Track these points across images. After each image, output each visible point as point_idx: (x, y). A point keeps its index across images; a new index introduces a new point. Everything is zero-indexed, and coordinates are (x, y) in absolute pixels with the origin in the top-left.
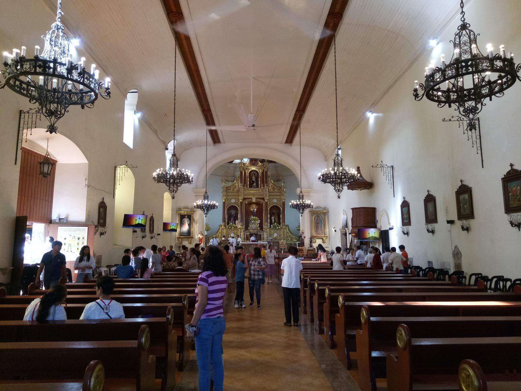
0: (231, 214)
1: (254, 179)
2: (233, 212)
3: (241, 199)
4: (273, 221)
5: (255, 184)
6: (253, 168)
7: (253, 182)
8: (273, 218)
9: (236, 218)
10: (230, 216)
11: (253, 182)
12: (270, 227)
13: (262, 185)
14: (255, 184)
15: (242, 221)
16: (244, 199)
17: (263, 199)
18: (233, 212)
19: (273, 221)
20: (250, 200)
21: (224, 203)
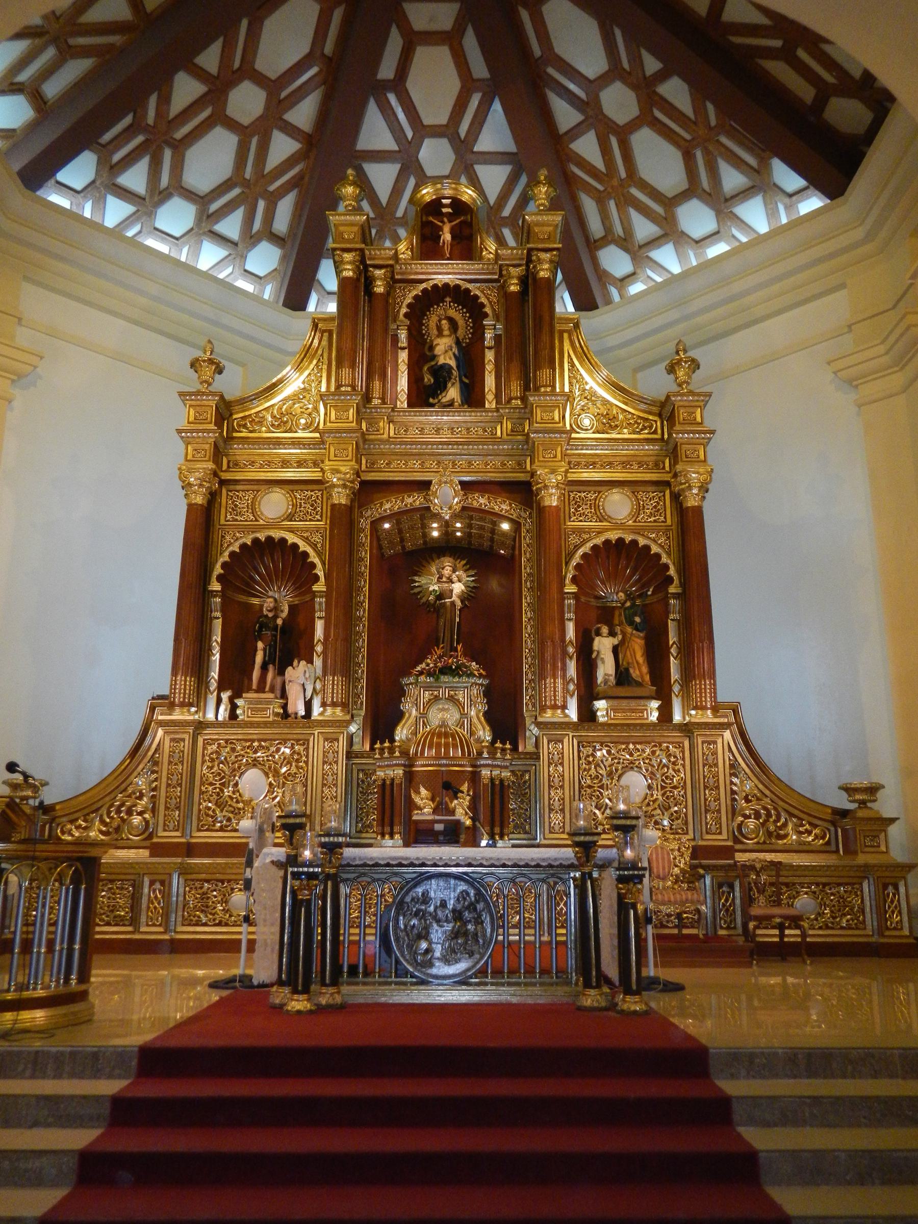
0: (235, 608)
1: (445, 351)
2: (275, 600)
3: (339, 472)
4: (606, 669)
5: (453, 393)
6: (445, 273)
7: (442, 376)
8: (604, 645)
9: (290, 645)
10: (244, 631)
11: (442, 376)
12: (587, 715)
13: (516, 389)
14: (453, 393)
15: (340, 664)
16: (368, 490)
17: (523, 491)
18: (275, 600)
19: (606, 669)
20: (414, 500)
21: (202, 525)
